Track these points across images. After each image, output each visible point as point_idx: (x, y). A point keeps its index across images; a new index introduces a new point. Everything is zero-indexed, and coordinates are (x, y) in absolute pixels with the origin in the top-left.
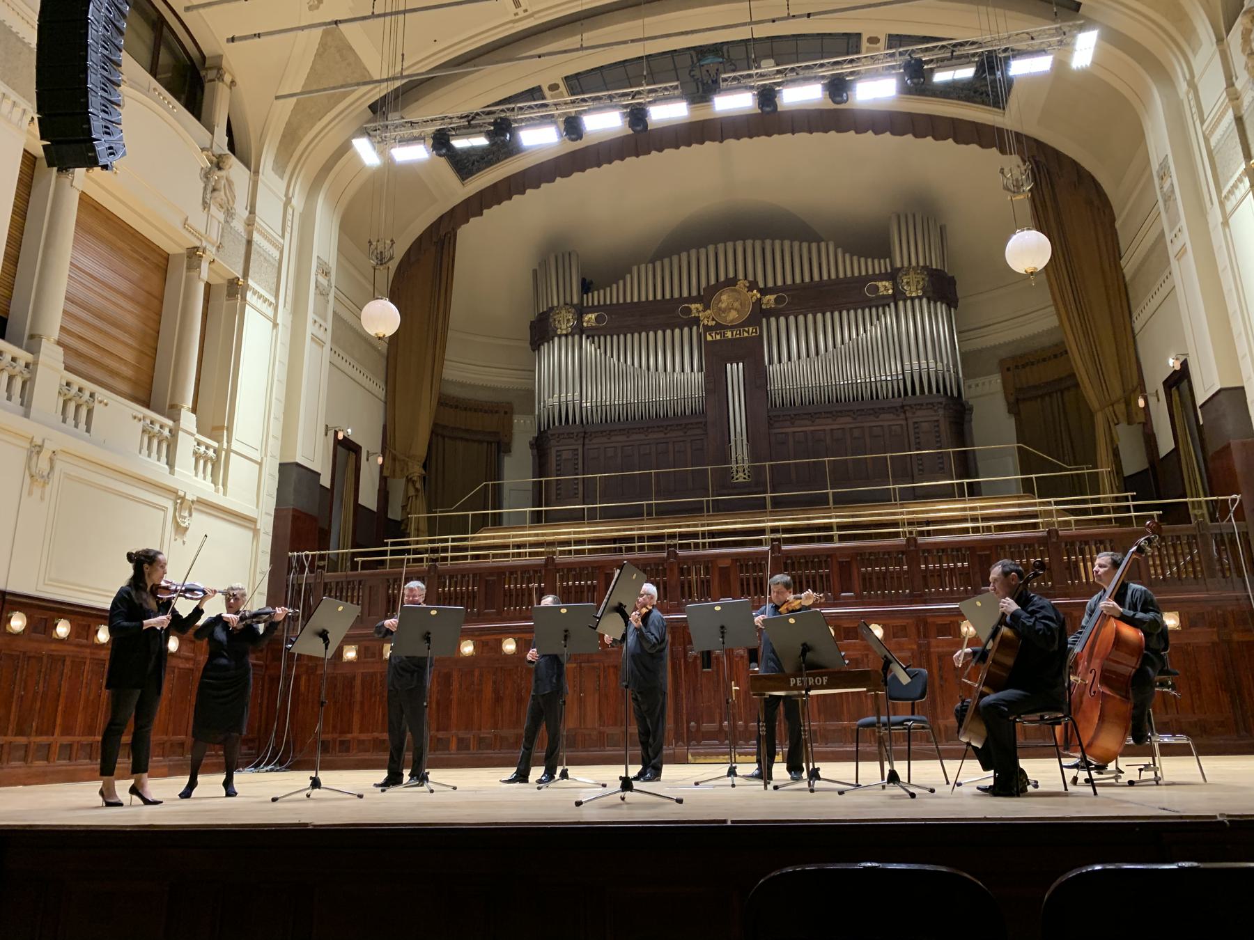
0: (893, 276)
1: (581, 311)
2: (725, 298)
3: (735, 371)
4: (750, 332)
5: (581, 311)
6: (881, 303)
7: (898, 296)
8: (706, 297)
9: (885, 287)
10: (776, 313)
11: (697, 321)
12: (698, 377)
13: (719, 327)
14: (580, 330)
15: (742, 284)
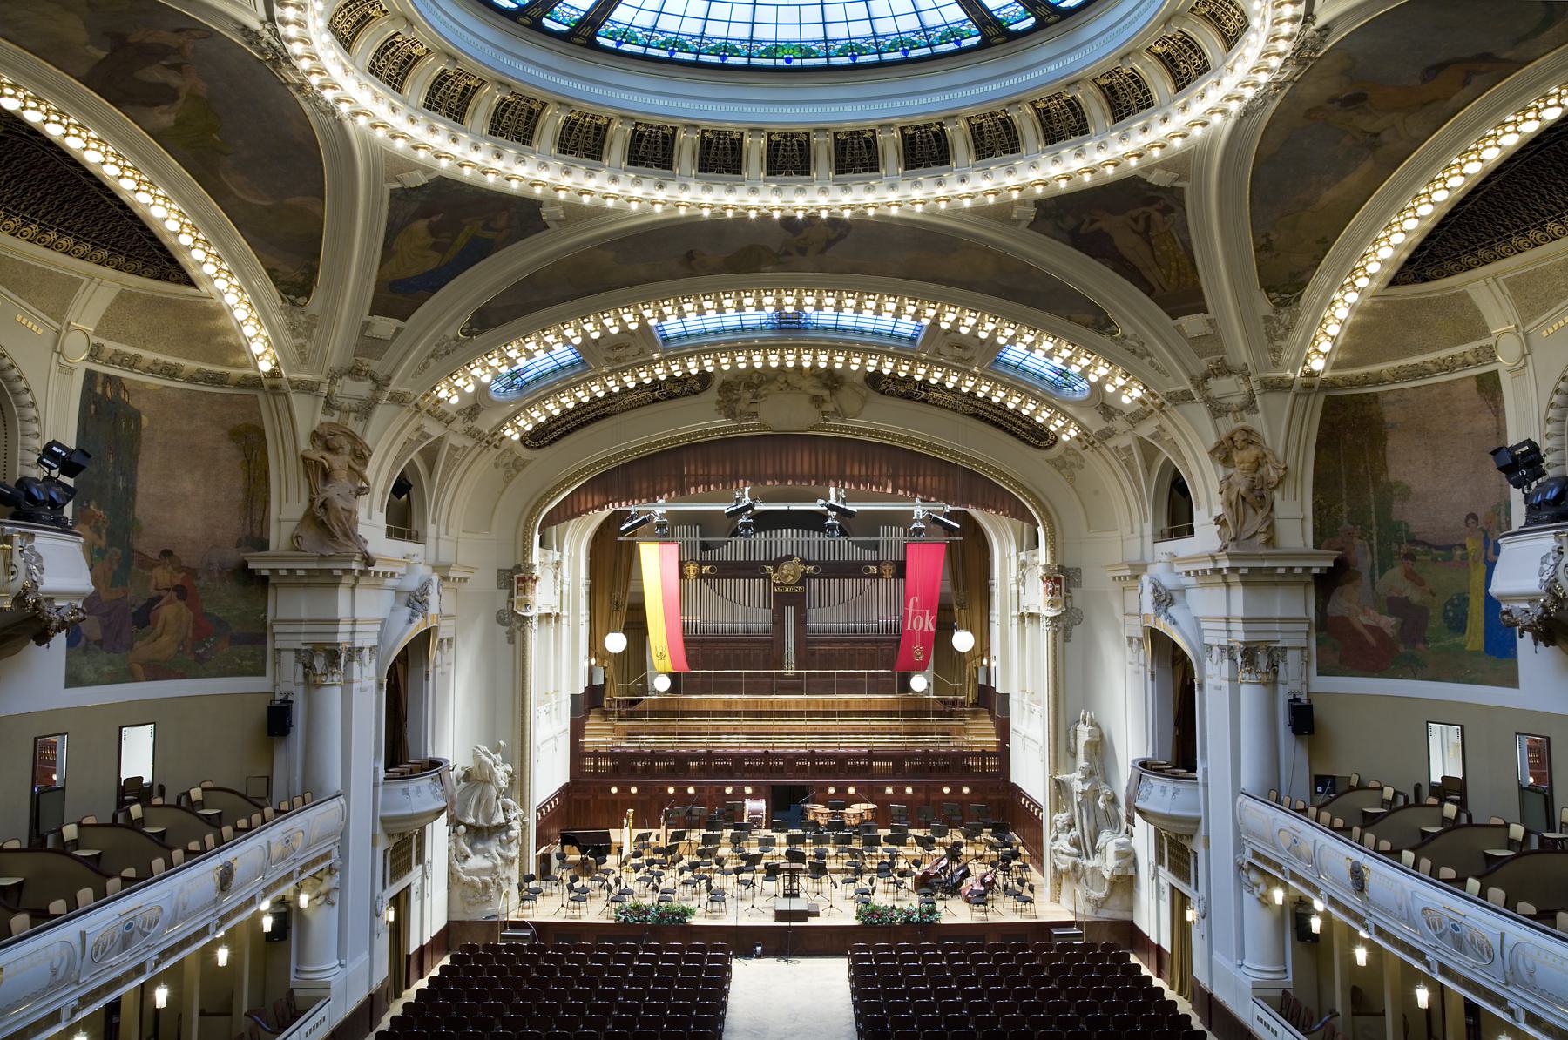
0: (877, 563)
1: (702, 563)
2: (786, 568)
3: (790, 612)
4: (799, 589)
5: (702, 563)
6: (873, 576)
7: (879, 576)
8: (777, 564)
9: (873, 569)
10: (814, 577)
11: (769, 577)
12: (769, 612)
13: (781, 584)
14: (700, 576)
15: (796, 560)
